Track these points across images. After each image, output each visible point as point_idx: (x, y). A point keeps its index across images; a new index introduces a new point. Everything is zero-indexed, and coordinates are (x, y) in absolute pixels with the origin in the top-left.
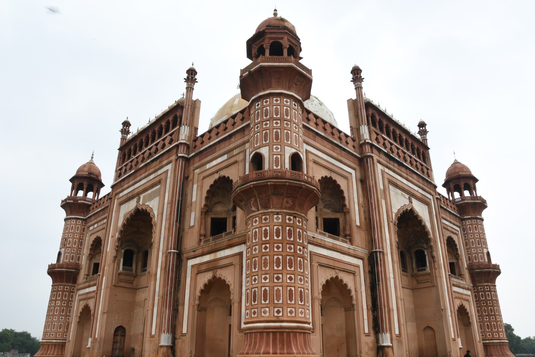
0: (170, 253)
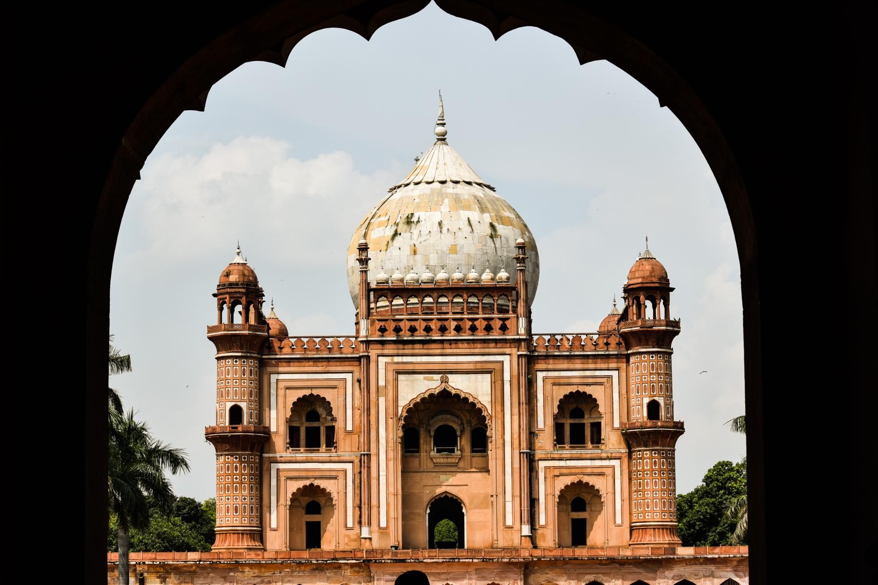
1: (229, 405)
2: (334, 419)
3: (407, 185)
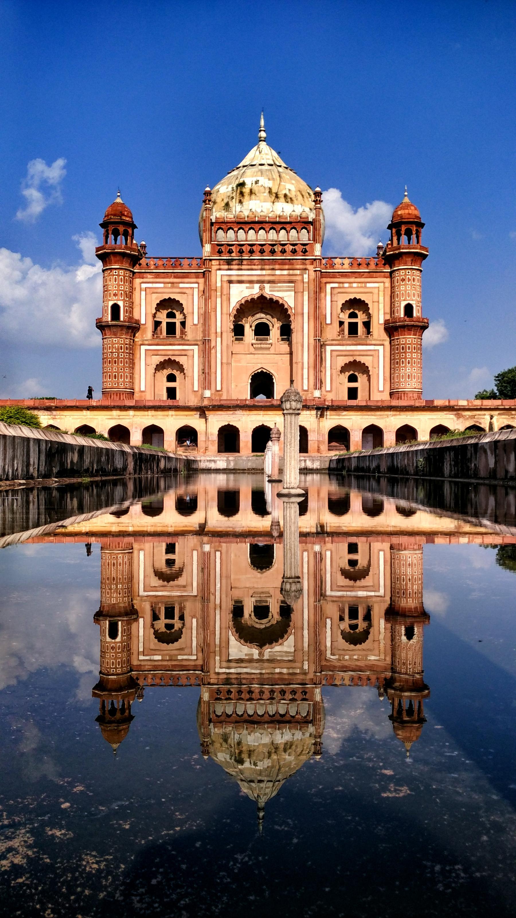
0: (319, 340)
1: (111, 303)
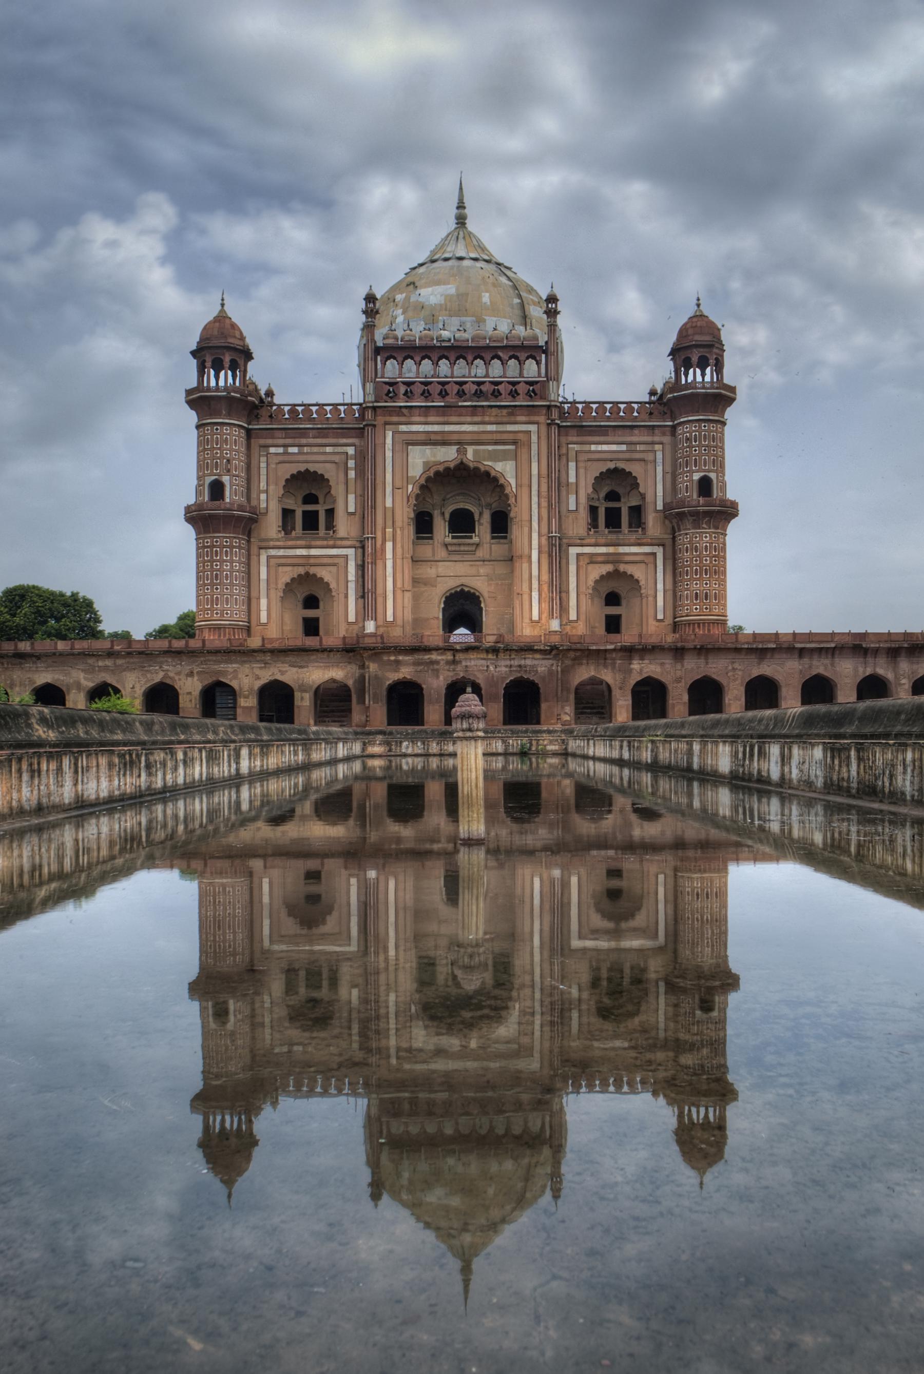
1: (209, 480)
2: (334, 502)
3: (421, 265)
